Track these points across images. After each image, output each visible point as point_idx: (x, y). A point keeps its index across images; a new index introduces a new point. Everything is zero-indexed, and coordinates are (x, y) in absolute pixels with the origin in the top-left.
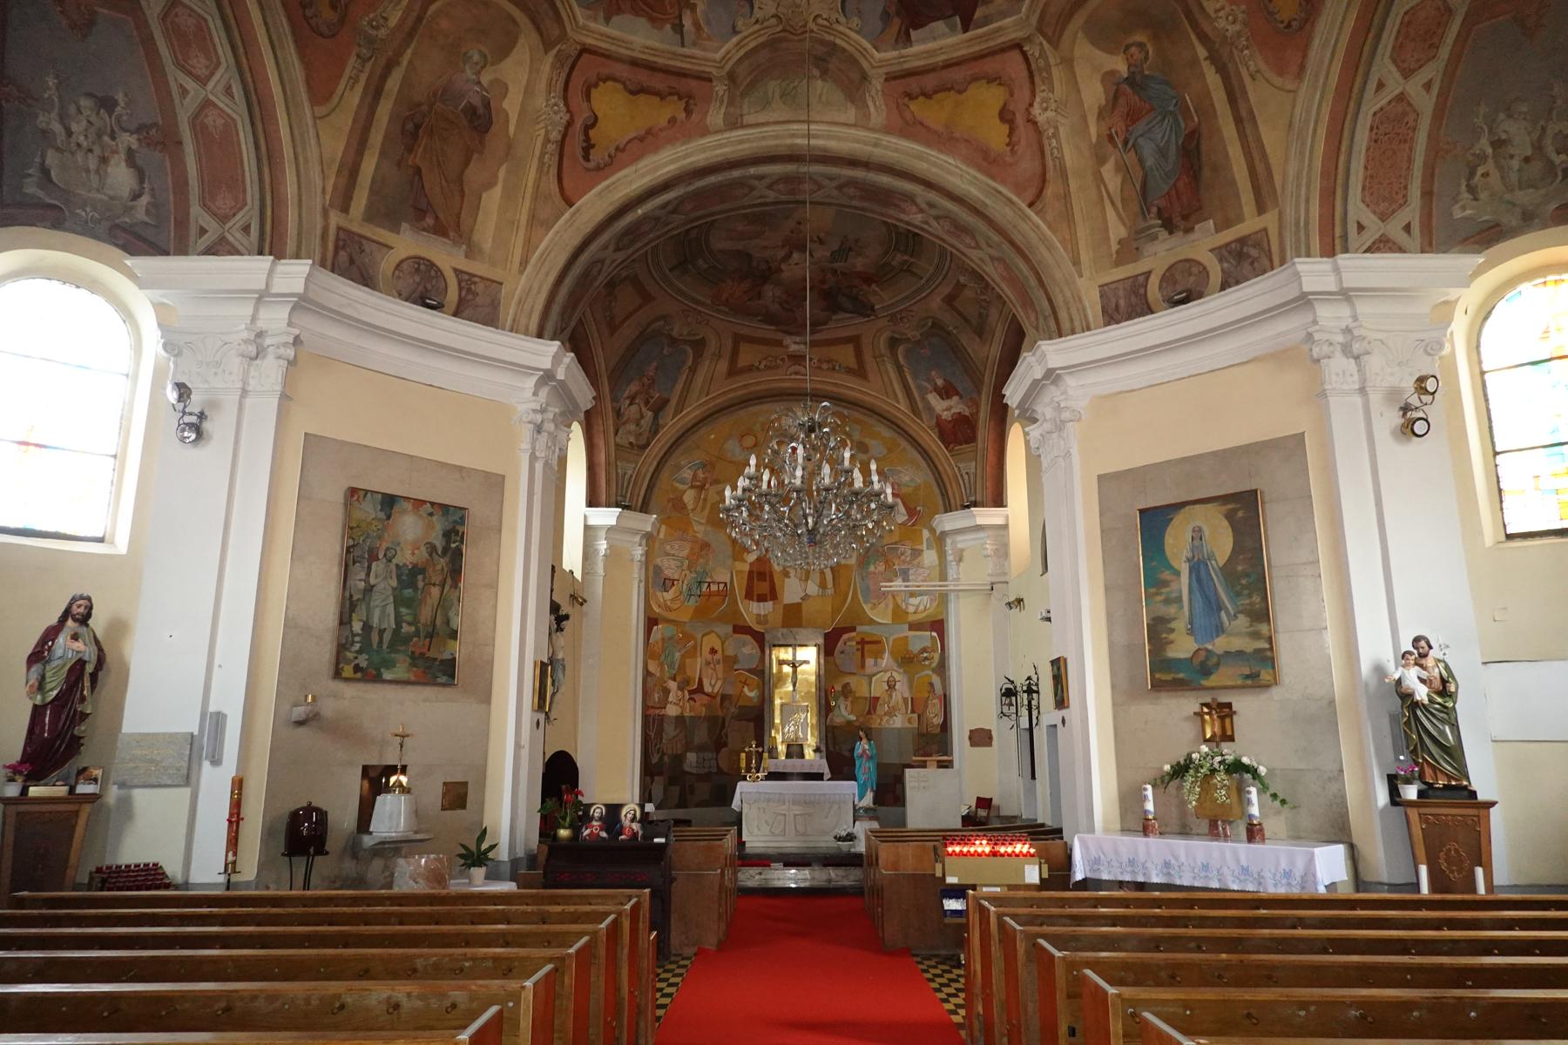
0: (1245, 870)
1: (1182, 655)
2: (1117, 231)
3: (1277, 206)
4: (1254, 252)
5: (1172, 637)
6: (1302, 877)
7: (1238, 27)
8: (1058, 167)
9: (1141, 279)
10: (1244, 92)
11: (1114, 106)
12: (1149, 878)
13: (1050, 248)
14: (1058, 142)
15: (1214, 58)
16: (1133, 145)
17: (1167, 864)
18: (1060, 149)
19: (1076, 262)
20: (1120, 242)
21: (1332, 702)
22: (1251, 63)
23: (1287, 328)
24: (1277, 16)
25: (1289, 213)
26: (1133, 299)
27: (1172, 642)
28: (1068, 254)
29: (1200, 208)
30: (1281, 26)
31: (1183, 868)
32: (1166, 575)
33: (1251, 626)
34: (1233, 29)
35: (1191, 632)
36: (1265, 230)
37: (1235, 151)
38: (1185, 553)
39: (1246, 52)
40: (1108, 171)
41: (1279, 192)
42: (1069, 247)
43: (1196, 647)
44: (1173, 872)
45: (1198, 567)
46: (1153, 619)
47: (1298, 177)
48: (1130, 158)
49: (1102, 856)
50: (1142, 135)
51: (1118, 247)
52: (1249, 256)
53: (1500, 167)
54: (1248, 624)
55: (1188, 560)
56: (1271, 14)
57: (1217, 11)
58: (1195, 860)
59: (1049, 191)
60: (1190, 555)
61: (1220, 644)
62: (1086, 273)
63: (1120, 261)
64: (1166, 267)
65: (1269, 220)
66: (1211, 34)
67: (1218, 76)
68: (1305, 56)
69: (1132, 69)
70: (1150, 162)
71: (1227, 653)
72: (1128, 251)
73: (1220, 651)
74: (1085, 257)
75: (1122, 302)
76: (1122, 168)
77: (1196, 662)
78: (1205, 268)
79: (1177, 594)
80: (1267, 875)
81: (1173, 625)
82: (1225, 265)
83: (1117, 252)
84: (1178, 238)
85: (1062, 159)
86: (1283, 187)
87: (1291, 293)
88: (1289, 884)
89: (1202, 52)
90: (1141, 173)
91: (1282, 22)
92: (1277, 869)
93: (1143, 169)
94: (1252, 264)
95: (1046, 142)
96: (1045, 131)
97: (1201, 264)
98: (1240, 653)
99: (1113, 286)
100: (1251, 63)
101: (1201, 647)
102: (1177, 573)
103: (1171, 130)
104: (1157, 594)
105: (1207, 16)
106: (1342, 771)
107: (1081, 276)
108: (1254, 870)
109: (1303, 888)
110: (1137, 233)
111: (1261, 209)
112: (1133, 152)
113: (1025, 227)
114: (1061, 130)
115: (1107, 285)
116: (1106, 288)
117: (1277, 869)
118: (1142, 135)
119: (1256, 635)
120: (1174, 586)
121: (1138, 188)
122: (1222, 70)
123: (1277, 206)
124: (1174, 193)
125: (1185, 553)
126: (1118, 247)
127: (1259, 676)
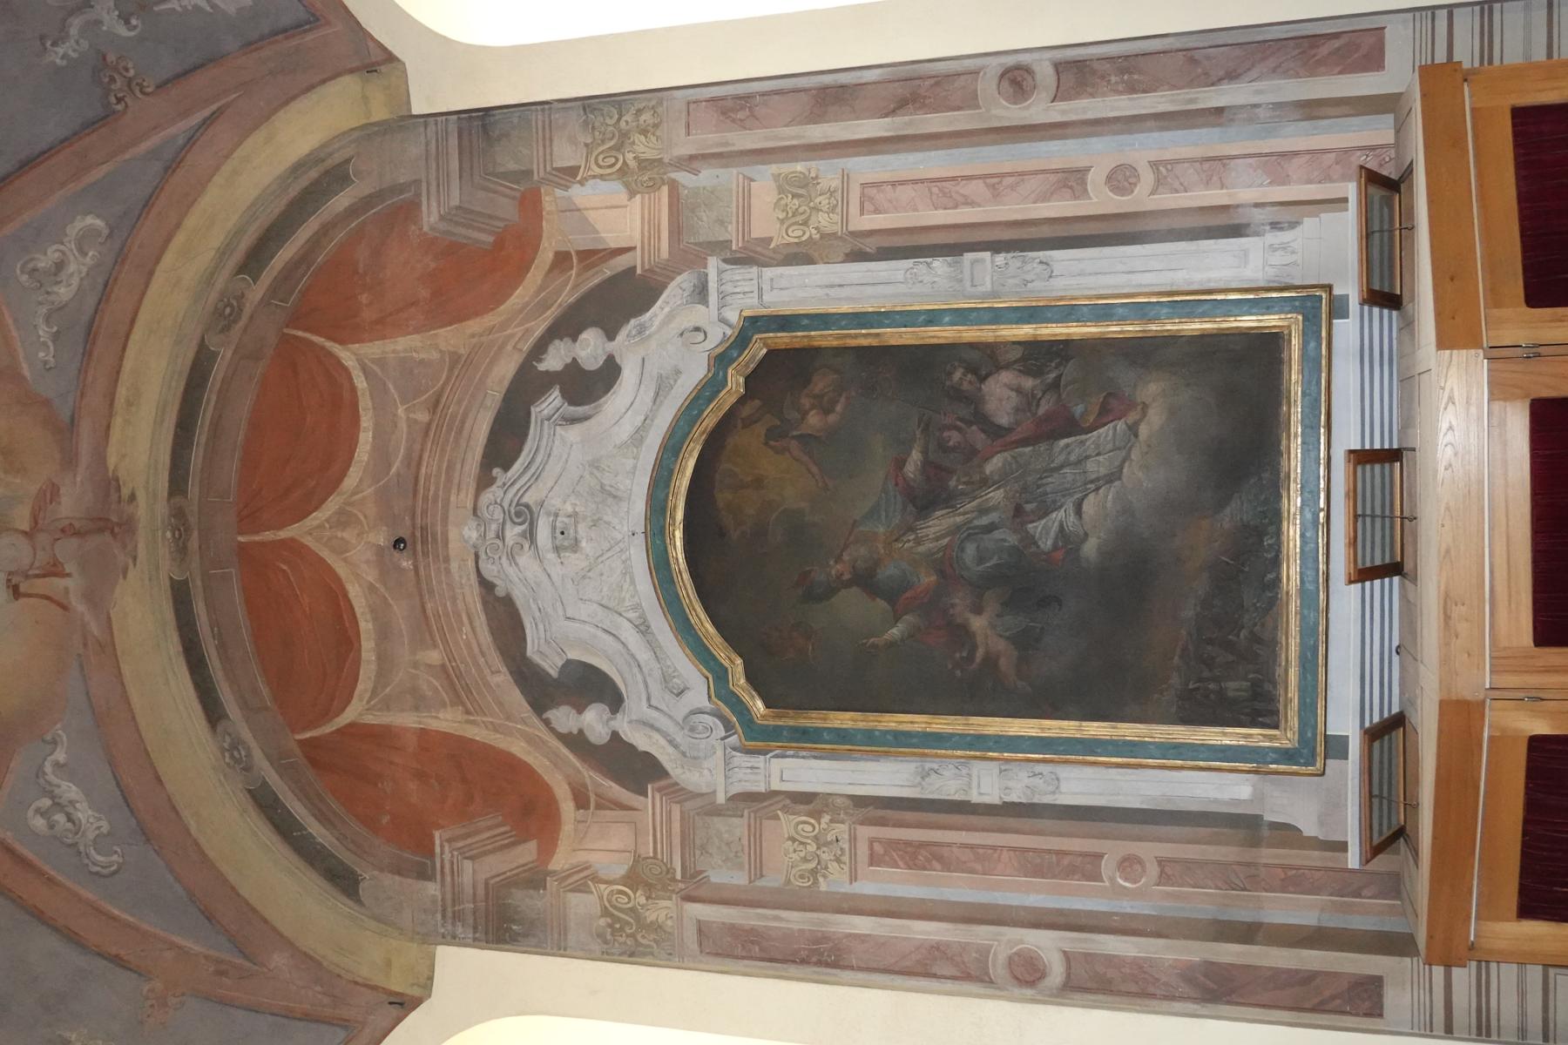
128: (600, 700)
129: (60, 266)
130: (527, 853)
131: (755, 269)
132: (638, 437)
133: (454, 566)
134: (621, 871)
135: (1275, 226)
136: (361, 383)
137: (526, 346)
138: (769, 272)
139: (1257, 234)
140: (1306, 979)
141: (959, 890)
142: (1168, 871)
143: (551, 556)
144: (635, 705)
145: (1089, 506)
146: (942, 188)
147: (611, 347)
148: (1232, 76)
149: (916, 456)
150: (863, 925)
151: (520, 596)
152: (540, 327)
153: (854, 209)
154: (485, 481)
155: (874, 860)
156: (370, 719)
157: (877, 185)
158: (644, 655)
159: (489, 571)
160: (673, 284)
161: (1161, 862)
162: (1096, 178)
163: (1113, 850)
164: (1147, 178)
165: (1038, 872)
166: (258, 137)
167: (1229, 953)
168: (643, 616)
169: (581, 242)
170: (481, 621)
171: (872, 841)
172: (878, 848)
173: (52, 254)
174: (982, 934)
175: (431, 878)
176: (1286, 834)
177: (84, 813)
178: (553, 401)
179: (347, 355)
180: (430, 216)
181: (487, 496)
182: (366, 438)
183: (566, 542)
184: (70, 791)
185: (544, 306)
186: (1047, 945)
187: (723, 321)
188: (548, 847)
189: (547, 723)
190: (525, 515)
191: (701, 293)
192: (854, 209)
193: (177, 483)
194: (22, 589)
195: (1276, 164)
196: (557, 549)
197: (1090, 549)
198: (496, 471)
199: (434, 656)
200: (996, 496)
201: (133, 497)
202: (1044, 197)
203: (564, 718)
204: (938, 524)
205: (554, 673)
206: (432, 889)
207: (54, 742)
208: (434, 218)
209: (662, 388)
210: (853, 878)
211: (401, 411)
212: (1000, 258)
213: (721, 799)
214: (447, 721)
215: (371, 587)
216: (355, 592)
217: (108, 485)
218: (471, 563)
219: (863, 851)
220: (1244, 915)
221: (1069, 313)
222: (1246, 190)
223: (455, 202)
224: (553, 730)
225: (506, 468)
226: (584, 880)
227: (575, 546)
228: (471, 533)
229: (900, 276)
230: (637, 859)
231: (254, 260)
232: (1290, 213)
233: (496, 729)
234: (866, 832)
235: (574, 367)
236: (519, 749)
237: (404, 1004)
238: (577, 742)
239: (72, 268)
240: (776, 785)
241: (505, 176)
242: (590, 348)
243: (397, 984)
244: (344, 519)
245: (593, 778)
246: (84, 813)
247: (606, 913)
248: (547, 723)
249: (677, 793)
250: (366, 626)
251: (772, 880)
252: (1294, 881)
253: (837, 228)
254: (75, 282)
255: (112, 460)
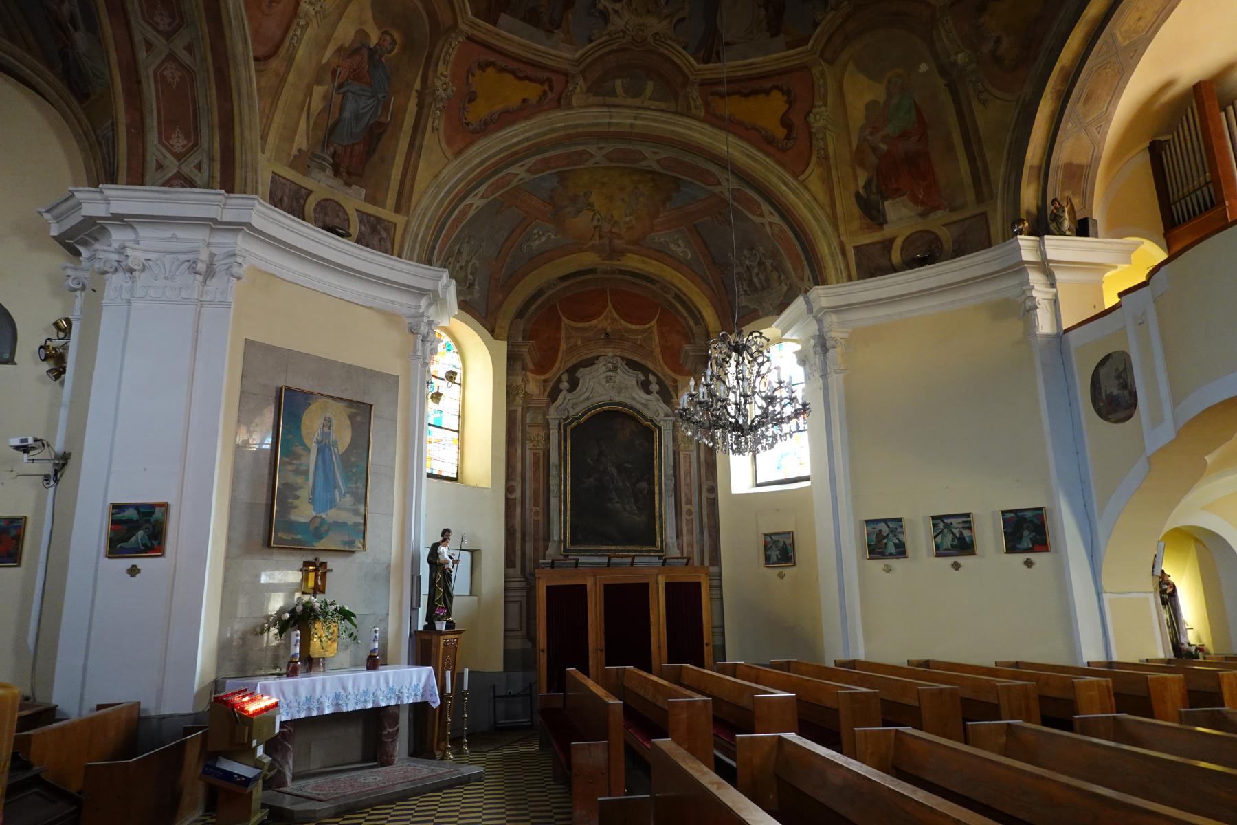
0: (391, 690)
1: (302, 520)
2: (301, 141)
3: (407, 213)
4: (384, 234)
5: (296, 502)
6: (423, 688)
7: (444, 95)
8: (290, 52)
9: (304, 192)
10: (424, 134)
11: (349, 56)
12: (378, 703)
13: (251, 107)
14: (303, 34)
15: (421, 95)
16: (344, 93)
17: (337, 696)
18: (299, 41)
19: (264, 137)
20: (300, 150)
21: (389, 566)
22: (437, 120)
23: (400, 302)
24: (466, 113)
25: (414, 225)
26: (294, 204)
27: (295, 507)
28: (261, 123)
29: (361, 176)
30: (464, 121)
31: (349, 697)
32: (299, 449)
33: (354, 504)
34: (440, 92)
35: (312, 501)
36: (395, 225)
37: (399, 160)
38: (316, 436)
39: (438, 112)
40: (319, 91)
41: (412, 208)
42: (264, 120)
43: (314, 514)
44: (341, 702)
45: (324, 448)
46: (283, 485)
47: (427, 209)
48: (337, 99)
49: (282, 700)
50: (353, 93)
51: (297, 153)
52: (380, 234)
53: (454, 263)
54: (352, 503)
55: (318, 442)
56: (464, 109)
57: (442, 74)
58: (359, 690)
59: (274, 64)
60: (320, 438)
61: (331, 515)
62: (268, 154)
63: (292, 165)
64: (324, 197)
65: (400, 220)
66: (429, 82)
67: (416, 108)
68: (466, 147)
69: (378, 48)
70: (347, 114)
71: (336, 523)
72: (302, 162)
73: (330, 521)
74: (272, 139)
75: (286, 199)
76: (327, 98)
77: (312, 527)
78: (348, 219)
79: (305, 468)
80: (405, 690)
81: (298, 493)
82: (363, 228)
83: (295, 157)
84: (338, 183)
85: (295, 49)
86: (415, 208)
87: (427, 285)
88: (416, 695)
89: (417, 85)
90: (337, 116)
91: (466, 119)
92: (410, 685)
93: (340, 115)
94: (380, 240)
95: (294, 26)
96: (300, 17)
97: (347, 215)
98: (344, 524)
99: (283, 181)
100: (437, 120)
101: (318, 515)
102: (308, 450)
103: (371, 108)
104: (290, 464)
105: (435, 71)
106: (388, 615)
107: (263, 152)
108: (396, 688)
109: (423, 696)
110: (315, 156)
111: (398, 210)
112: (341, 96)
113: (243, 72)
114: (309, 29)
115: (279, 176)
116: (277, 177)
117: (410, 685)
118: (353, 93)
119: (356, 512)
120: (304, 460)
121: (330, 124)
122: (420, 106)
123: (408, 216)
124: (349, 149)
125: (316, 436)
126: (297, 153)
127: (354, 543)
128: (570, 388)
129: (679, 246)
130: (531, 366)
131: (671, 428)
132: (634, 399)
133: (602, 349)
134: (528, 391)
135: (678, 545)
136: (647, 326)
137: (656, 372)
138: (671, 432)
139: (677, 541)
140: (514, 551)
141: (529, 474)
142: (536, 523)
143: (605, 376)
144: (569, 396)
145: (618, 505)
146: (688, 473)
147: (655, 392)
148: (710, 536)
149: (630, 466)
150: (519, 451)
151: (595, 367)
152: (660, 375)
153: (684, 452)
154: (623, 358)
155: (535, 454)
156: (563, 325)
157: (690, 458)
158: (582, 398)
159: (601, 359)
160: (669, 409)
161: (538, 521)
162: (689, 507)
163: (540, 509)
164: (689, 518)
165: (534, 493)
166: (709, 304)
167: (519, 535)
168: (590, 399)
169: (679, 386)
170: (589, 356)
171: (539, 454)
172: (538, 455)
173: (682, 244)
174: (519, 479)
175: (523, 339)
176: (546, 548)
177: (537, 242)
178: (642, 377)
179: (654, 322)
180: (687, 347)
181: (618, 358)
182: (633, 327)
183: (608, 379)
184: (543, 239)
185: (665, 376)
186: (517, 495)
187: (660, 421)
188: (533, 372)
189: (564, 373)
190: (615, 369)
191: (667, 415)
192: (684, 452)
193: (622, 272)
194: (596, 229)
195: (691, 545)
196: (607, 377)
197: (609, 505)
198: (625, 362)
199: (579, 343)
200: (621, 484)
201: (619, 260)
202: (686, 495)
203: (565, 377)
204: (614, 471)
205: (576, 375)
206: (520, 340)
207: (556, 235)
208: (686, 348)
209: (645, 405)
210: (530, 449)
211: (640, 337)
212: (673, 486)
213: (547, 417)
214: (563, 346)
215: (596, 327)
216: (595, 322)
217: (622, 253)
218: (603, 354)
219: (538, 452)
220: (527, 538)
221: (661, 501)
222: (685, 539)
223: (690, 353)
224: (562, 374)
225: (626, 364)
226: (525, 381)
227: (607, 382)
228: (610, 354)
229: (669, 463)
230: (531, 395)
231: (678, 298)
232: (680, 547)
233: (562, 359)
234: (541, 452)
235: (650, 383)
236: (557, 365)
237: (492, 332)
238: (559, 380)
239: (678, 249)
240: (551, 431)
241: (696, 368)
242: (655, 387)
243: (497, 330)
244: (613, 320)
245: (551, 384)
246: (537, 242)
247: (517, 386)
248: (564, 373)
249: (548, 406)
250: (586, 324)
251: (528, 429)
252: (536, 549)
253: (680, 448)
254: (675, 249)
255: (629, 255)
